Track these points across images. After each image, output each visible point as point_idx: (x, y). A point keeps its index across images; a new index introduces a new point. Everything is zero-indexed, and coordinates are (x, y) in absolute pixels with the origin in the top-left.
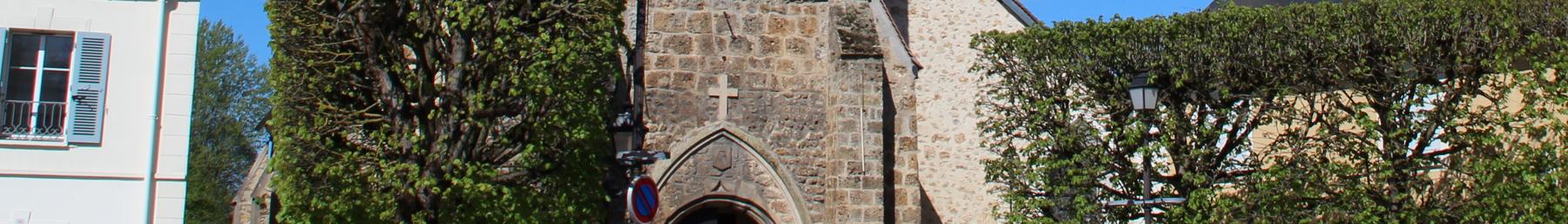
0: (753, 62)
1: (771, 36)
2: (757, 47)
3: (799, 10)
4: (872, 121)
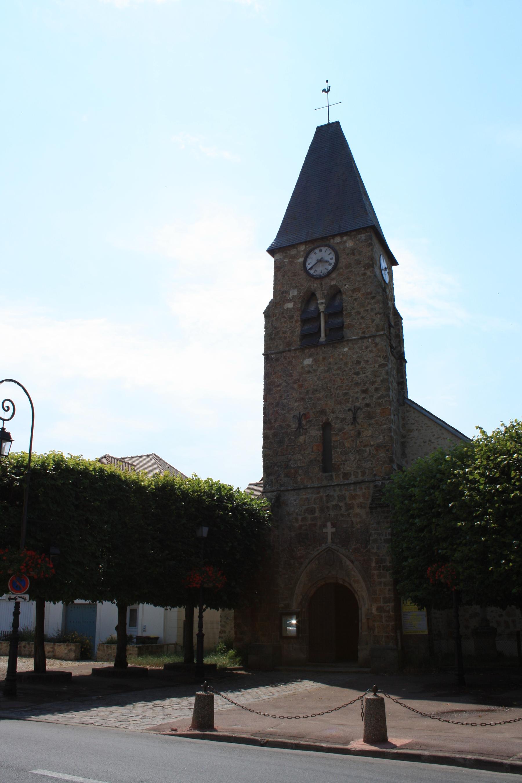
0: (342, 515)
1: (350, 502)
2: (343, 509)
3: (362, 489)
4: (385, 538)
